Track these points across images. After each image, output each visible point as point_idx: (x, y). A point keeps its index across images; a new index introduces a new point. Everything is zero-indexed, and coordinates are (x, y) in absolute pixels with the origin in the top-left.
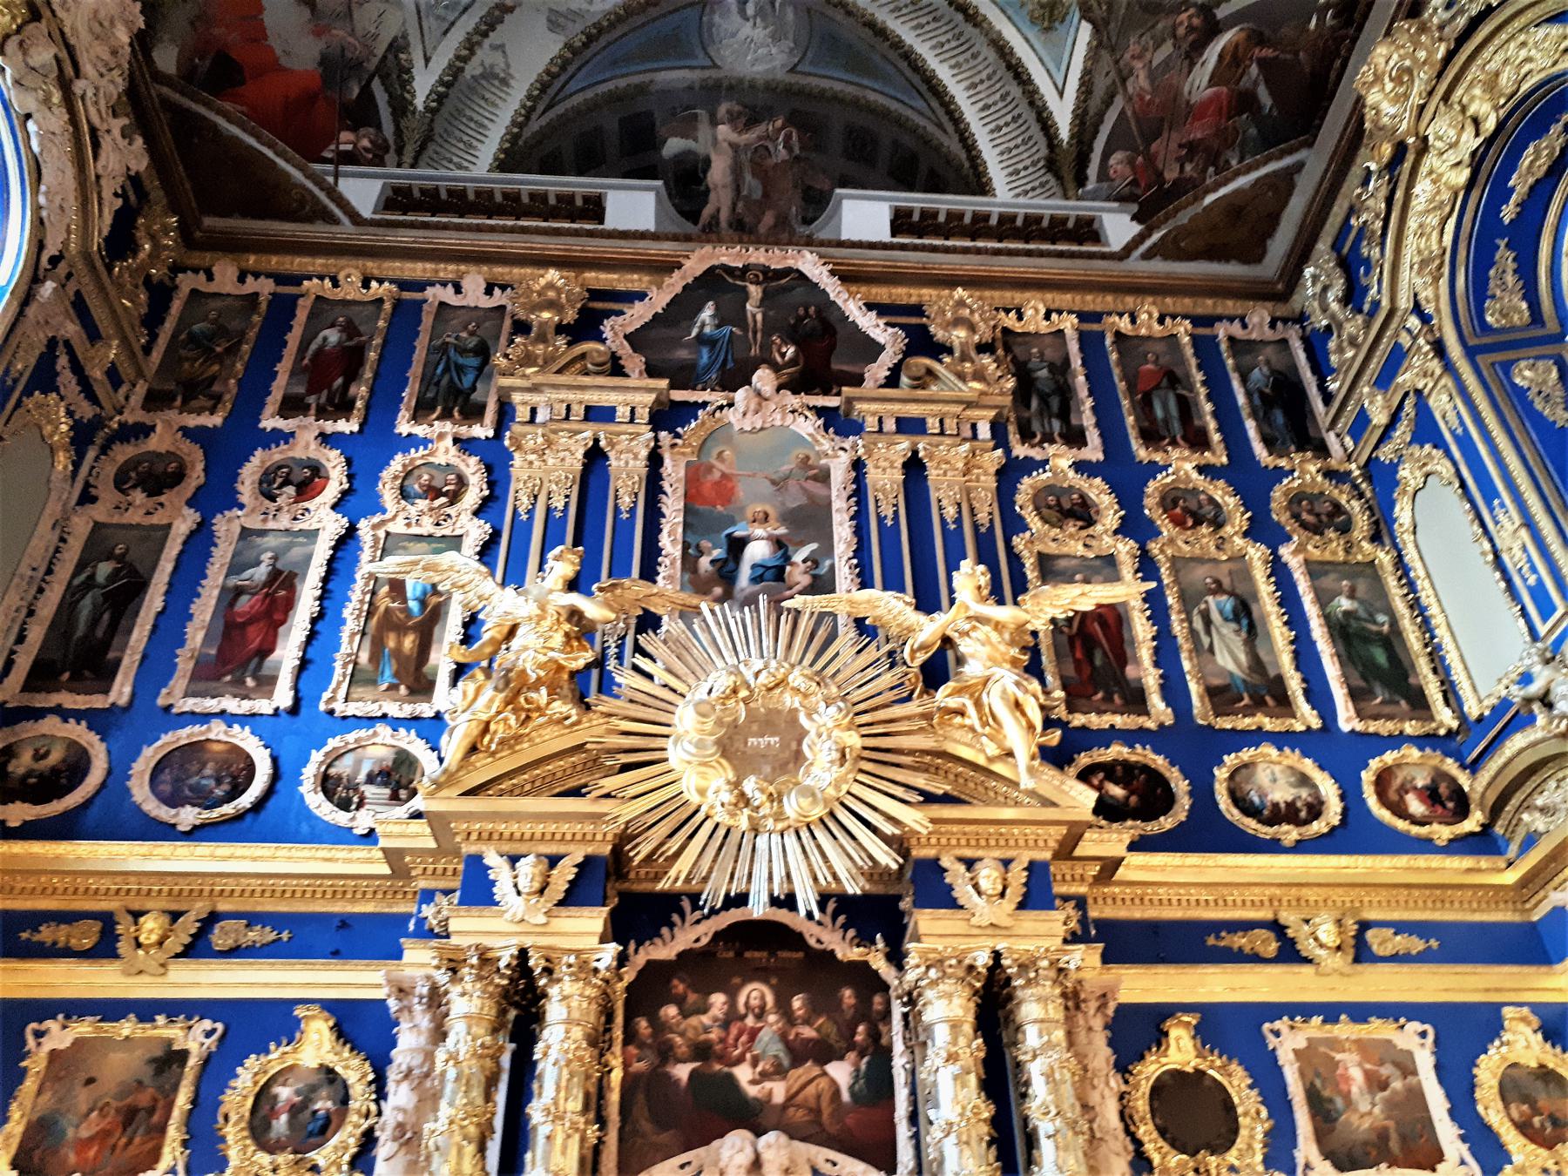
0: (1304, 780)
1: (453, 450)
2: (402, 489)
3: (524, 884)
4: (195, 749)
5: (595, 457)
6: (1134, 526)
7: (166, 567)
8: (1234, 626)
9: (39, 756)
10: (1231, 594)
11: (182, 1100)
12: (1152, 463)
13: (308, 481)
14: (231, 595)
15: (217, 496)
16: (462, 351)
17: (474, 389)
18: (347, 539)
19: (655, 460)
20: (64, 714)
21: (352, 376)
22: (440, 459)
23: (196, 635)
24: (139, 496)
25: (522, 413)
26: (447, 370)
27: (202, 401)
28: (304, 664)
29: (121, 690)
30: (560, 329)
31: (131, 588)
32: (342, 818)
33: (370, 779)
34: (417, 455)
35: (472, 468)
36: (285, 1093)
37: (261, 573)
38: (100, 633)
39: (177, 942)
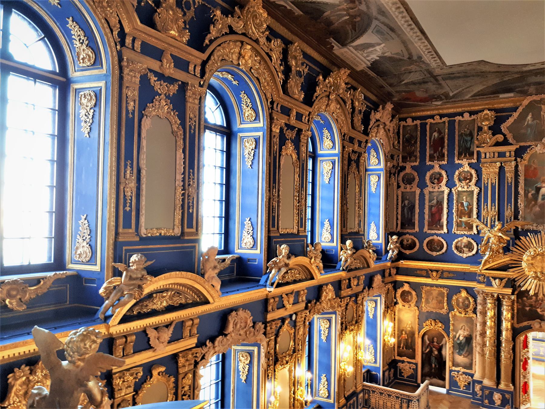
1: (468, 167)
2: (459, 178)
3: (497, 284)
4: (432, 240)
5: (501, 168)
7: (417, 202)
9: (408, 241)
11: (446, 299)
13: (438, 178)
14: (431, 207)
15: (422, 185)
16: (466, 135)
17: (470, 147)
18: (450, 194)
19: (517, 166)
20: (410, 234)
21: (443, 147)
22: (466, 170)
23: (426, 217)
24: (408, 186)
25: (483, 155)
26: (463, 142)
27: (413, 158)
28: (448, 222)
29: (417, 229)
30: (490, 128)
31: (412, 208)
32: (461, 255)
33: (464, 247)
34: (461, 169)
35: (473, 172)
36: (460, 300)
37: (435, 202)
38: (410, 216)
39: (438, 276)
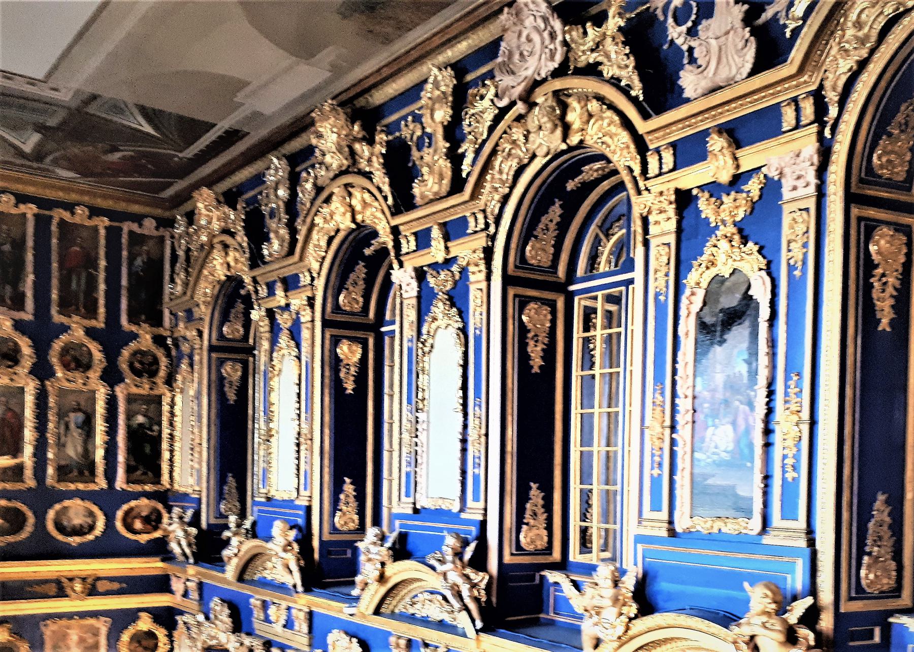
0: (91, 514)
6: (42, 371)
8: (80, 431)
10: (84, 412)
12: (62, 324)
